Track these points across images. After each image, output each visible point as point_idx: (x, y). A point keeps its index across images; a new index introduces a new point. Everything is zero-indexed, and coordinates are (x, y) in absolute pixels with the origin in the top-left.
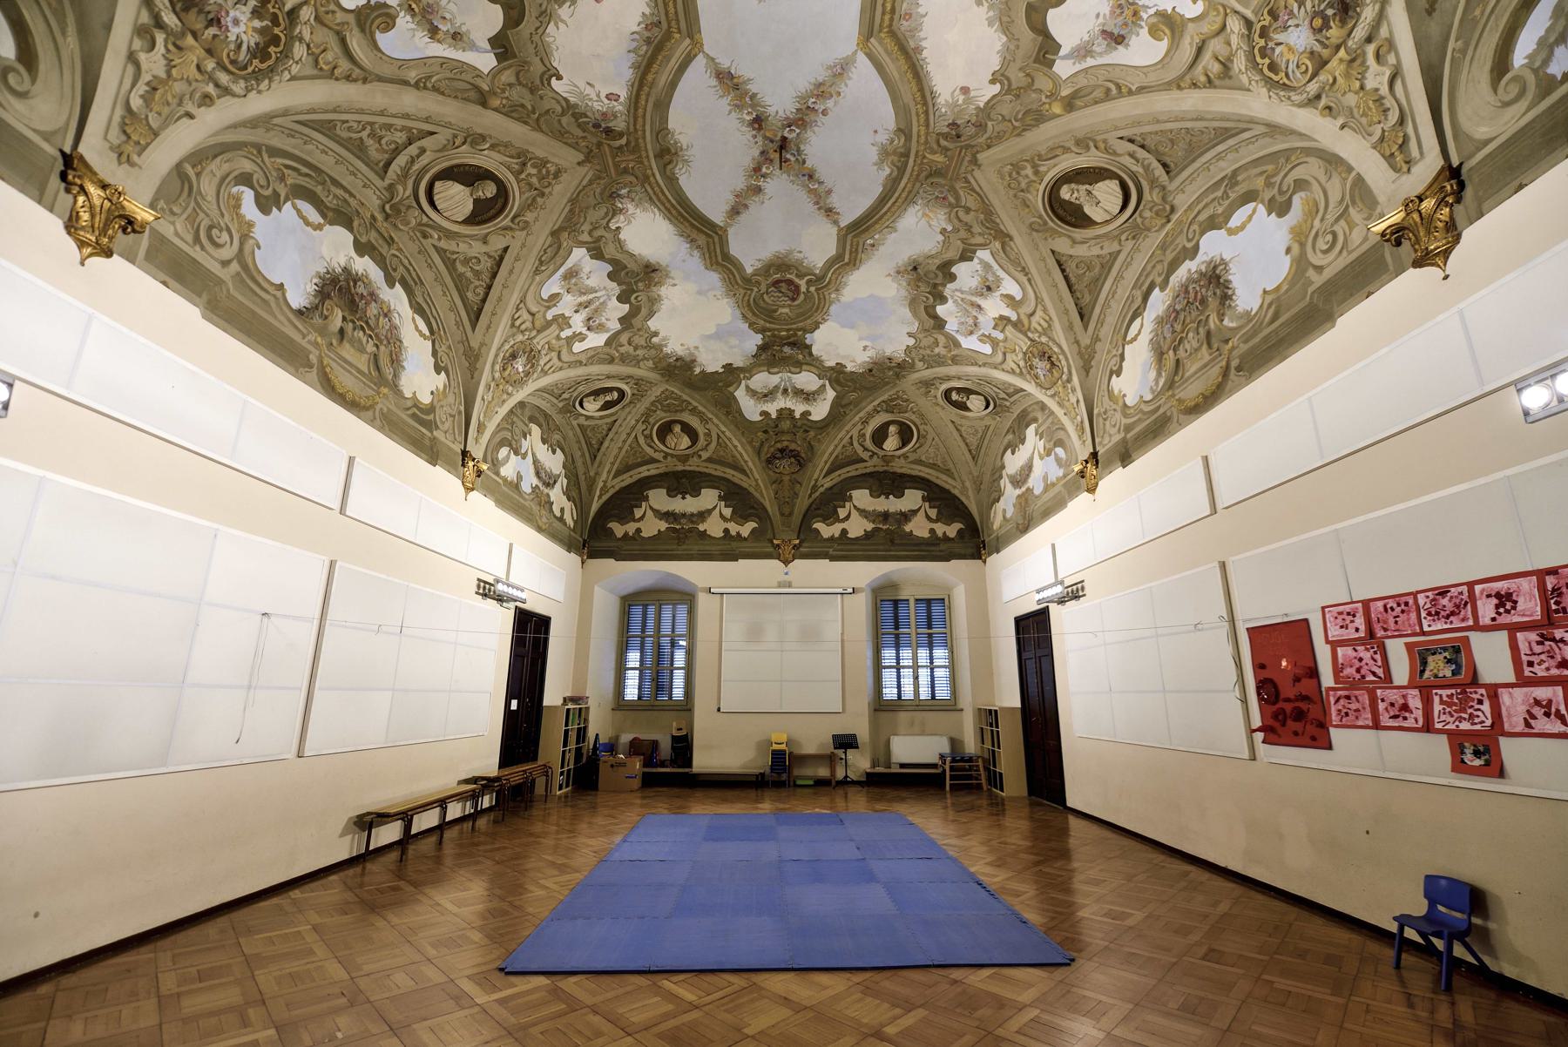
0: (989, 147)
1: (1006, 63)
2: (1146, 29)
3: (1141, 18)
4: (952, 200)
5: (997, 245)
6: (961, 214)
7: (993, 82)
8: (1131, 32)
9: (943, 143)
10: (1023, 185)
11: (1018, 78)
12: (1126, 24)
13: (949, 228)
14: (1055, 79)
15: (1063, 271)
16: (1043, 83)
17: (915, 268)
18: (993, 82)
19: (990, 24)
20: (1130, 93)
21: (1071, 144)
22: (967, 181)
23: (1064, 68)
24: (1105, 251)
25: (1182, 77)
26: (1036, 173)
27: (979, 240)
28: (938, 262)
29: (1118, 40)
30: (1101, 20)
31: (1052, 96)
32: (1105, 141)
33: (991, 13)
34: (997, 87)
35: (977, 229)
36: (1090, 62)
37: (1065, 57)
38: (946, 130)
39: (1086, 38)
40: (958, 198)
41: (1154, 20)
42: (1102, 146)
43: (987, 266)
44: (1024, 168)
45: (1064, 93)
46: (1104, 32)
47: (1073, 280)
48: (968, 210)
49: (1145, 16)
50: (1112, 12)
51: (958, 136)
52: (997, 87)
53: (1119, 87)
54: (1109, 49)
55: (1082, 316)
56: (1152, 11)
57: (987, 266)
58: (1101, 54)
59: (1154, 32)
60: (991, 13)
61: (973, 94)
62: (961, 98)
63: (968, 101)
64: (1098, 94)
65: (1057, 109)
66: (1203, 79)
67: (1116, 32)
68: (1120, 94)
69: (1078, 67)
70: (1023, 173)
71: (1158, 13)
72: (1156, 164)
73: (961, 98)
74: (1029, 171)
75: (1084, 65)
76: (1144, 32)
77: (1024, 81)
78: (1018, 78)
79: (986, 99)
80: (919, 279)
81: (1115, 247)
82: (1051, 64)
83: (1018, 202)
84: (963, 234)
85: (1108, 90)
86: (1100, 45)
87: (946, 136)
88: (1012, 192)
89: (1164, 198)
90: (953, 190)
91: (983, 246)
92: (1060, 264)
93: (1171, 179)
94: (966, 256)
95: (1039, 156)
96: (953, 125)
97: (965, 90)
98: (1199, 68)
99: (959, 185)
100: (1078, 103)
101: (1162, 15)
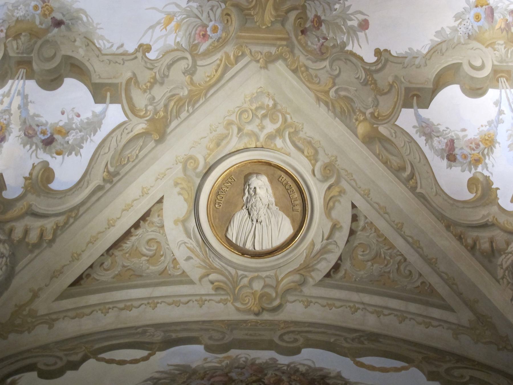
0: (295, 71)
1: (400, 60)
2: (470, 175)
3: (476, 167)
4: (204, 47)
5: (141, 126)
6: (182, 65)
7: (378, 52)
8: (462, 164)
9: (292, 16)
10: (248, 128)
11: (384, 79)
12: (465, 157)
13: (152, 55)
14: (394, 114)
15: (136, 226)
16: (385, 105)
17: (58, 24)
18: (378, 52)
19: (438, 33)
20: (413, 189)
21: (323, 159)
22: (237, 59)
23: (407, 119)
24: (184, 265)
25: (457, 224)
26: (271, 137)
27: (141, 100)
28: (81, 54)
29: (451, 157)
30: (461, 134)
31: (376, 118)
32: (342, 192)
33: (448, 31)
34: (370, 58)
35: (160, 93)
36: (421, 141)
37: (418, 116)
38: (311, 15)
39: (442, 128)
40: (207, 53)
41: (481, 179)
42: (335, 191)
43: (93, 125)
44: (273, 121)
45: (382, 129)
46: (452, 141)
47: (127, 245)
48: (191, 72)
49: (479, 169)
50: (471, 141)
51: (303, 32)
52: (370, 58)
53: (412, 176)
54: (440, 153)
55: (76, 283)
56: (486, 173)
57: (93, 125)
58: (432, 147)
59: (472, 183)
60: (448, 31)
61: (361, 34)
62: (354, 23)
63: (352, 32)
64: (395, 161)
65: (362, 129)
66: (470, 241)
67: (457, 151)
68: (406, 182)
69: (412, 132)
70: (267, 122)
71: (487, 178)
72: (333, 259)
73: (354, 23)
74: (270, 127)
75: (416, 137)
76: (468, 175)
77: (383, 84)
78: (384, 79)
79: (357, 50)
80: (35, 34)
81: (195, 274)
82: (408, 105)
83: (221, 130)
84: (145, 76)
85: (404, 169)
86: (440, 143)
87: (302, 17)
88: (233, 118)
89: (287, 291)
90: (222, 43)
91: (132, 109)
92: (144, 218)
93: (320, 284)
94: (100, 92)
95: (296, 132)
96: (318, 22)
97: (364, 25)
98: (474, 234)
99: (230, 50)
100: (377, 147)
101: (488, 182)
